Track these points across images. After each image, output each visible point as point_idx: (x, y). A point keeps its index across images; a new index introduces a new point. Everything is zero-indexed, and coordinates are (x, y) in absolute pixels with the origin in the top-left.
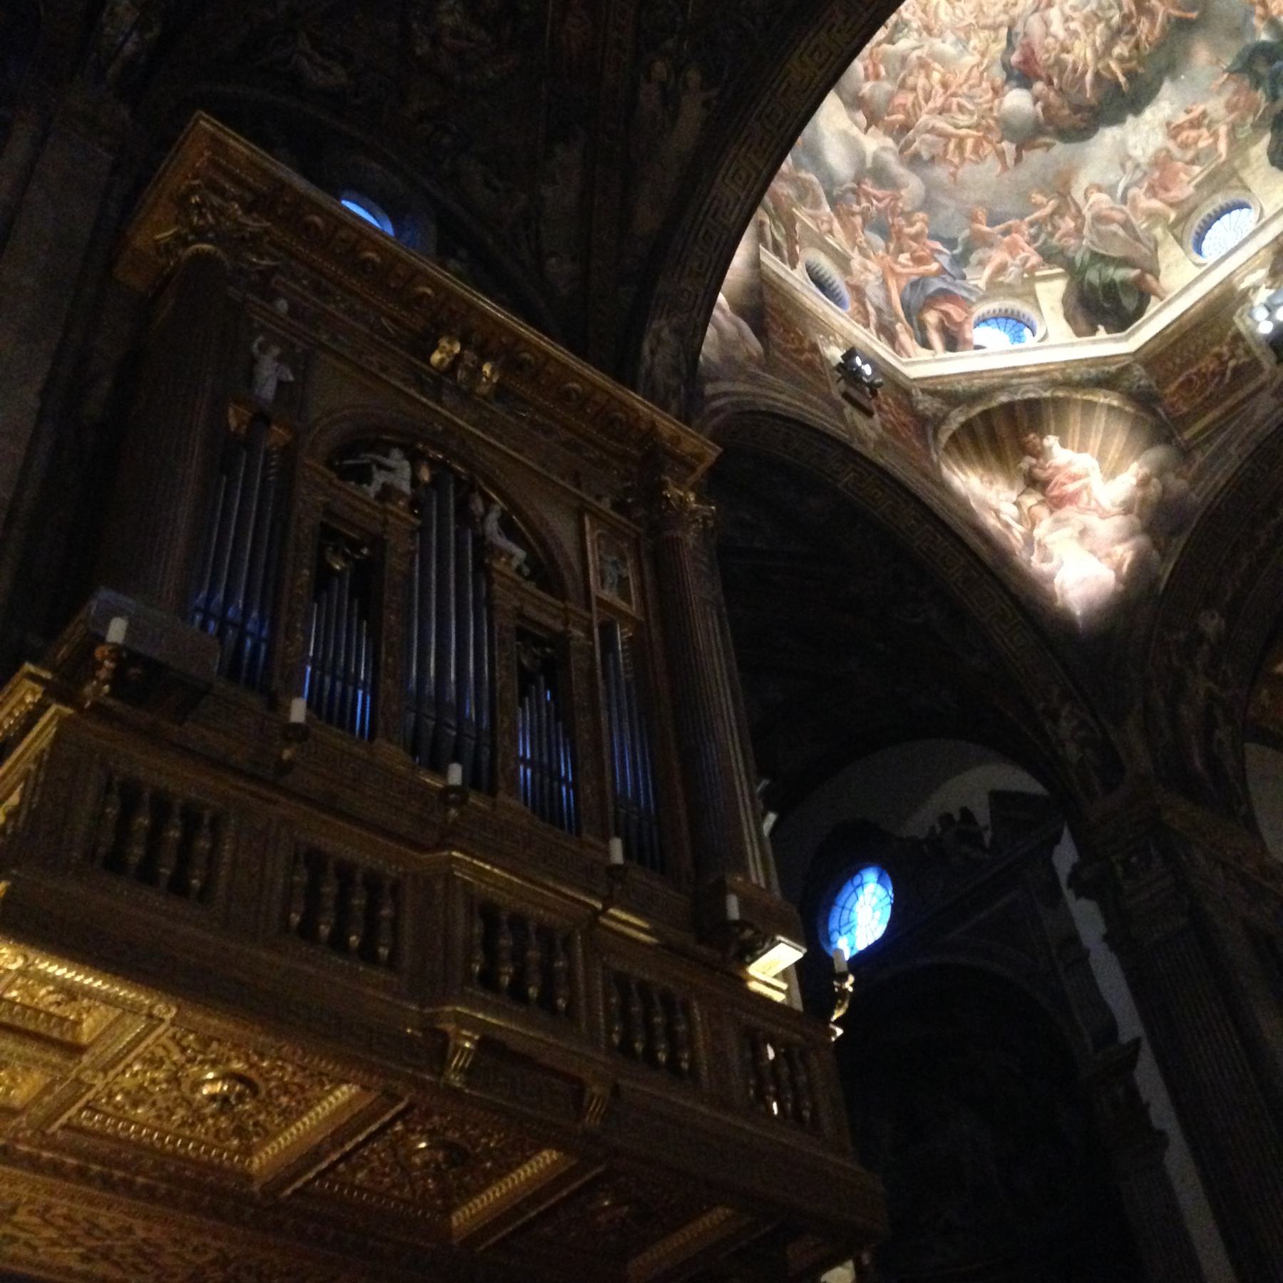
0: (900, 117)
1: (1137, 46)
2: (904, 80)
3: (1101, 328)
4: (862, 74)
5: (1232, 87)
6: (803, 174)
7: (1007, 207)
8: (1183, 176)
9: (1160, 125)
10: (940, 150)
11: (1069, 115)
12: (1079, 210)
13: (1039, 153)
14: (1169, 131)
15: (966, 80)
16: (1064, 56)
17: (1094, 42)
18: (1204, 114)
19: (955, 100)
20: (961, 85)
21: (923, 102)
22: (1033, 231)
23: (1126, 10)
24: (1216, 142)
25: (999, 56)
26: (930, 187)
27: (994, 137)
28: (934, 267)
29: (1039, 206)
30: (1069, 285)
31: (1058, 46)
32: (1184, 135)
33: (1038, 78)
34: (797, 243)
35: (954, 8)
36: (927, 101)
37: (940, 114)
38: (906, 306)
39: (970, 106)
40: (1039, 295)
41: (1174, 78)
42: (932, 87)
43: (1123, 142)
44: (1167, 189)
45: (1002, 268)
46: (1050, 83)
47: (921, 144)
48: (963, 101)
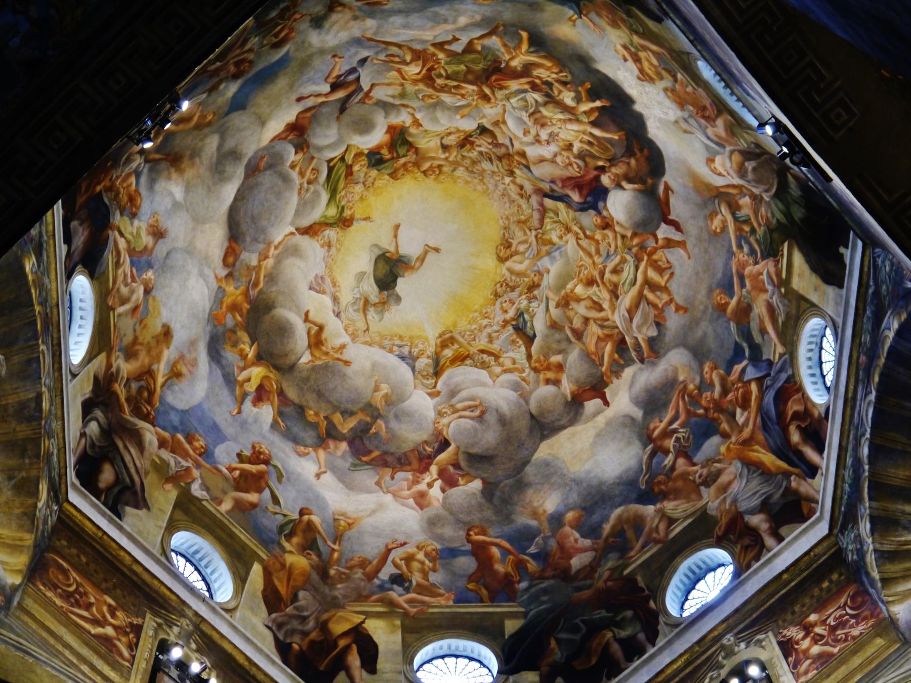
0: (609, 348)
1: (565, 84)
2: (574, 331)
3: (842, 250)
4: (551, 388)
5: (593, 15)
6: (607, 528)
7: (719, 263)
8: (689, 89)
9: (642, 86)
10: (652, 312)
11: (637, 160)
12: (734, 186)
13: (673, 201)
14: (646, 80)
15: (590, 255)
16: (575, 150)
17: (560, 120)
18: (625, 47)
19: (607, 275)
20: (594, 263)
21: (602, 314)
22: (746, 249)
23: (527, 87)
24: (651, 51)
25: (571, 212)
26: (682, 343)
27: (651, 243)
28: (754, 387)
29: (724, 228)
30: (801, 250)
31: (565, 154)
32: (649, 72)
33: (597, 179)
34: (647, 599)
35: (516, 253)
36: (601, 309)
37: (617, 297)
38: (780, 453)
39: (617, 259)
40: (801, 292)
41: (592, 59)
42: (589, 298)
43: (660, 120)
44: (704, 108)
45: (771, 309)
46: (602, 169)
47: (640, 332)
48: (610, 266)
